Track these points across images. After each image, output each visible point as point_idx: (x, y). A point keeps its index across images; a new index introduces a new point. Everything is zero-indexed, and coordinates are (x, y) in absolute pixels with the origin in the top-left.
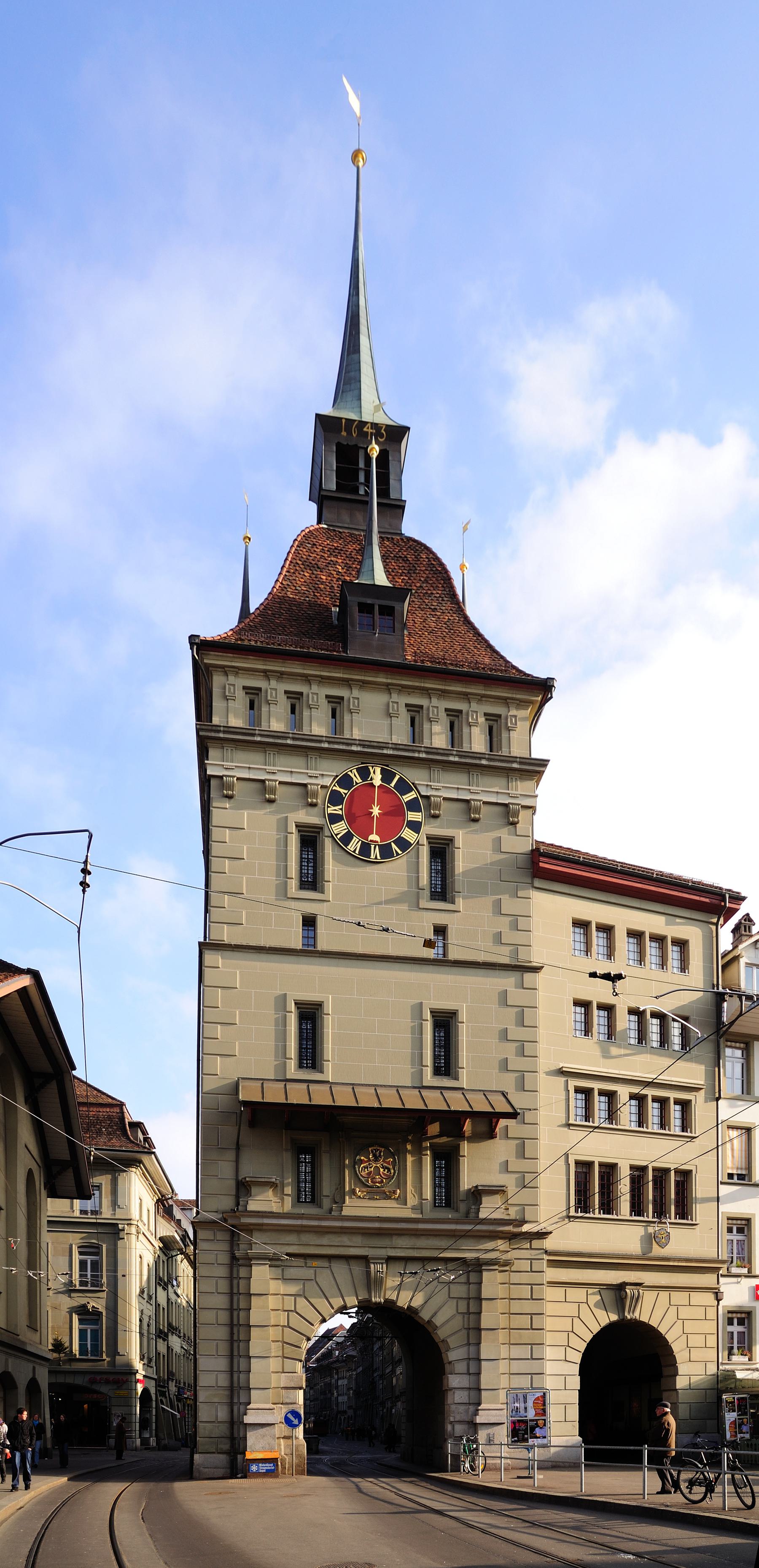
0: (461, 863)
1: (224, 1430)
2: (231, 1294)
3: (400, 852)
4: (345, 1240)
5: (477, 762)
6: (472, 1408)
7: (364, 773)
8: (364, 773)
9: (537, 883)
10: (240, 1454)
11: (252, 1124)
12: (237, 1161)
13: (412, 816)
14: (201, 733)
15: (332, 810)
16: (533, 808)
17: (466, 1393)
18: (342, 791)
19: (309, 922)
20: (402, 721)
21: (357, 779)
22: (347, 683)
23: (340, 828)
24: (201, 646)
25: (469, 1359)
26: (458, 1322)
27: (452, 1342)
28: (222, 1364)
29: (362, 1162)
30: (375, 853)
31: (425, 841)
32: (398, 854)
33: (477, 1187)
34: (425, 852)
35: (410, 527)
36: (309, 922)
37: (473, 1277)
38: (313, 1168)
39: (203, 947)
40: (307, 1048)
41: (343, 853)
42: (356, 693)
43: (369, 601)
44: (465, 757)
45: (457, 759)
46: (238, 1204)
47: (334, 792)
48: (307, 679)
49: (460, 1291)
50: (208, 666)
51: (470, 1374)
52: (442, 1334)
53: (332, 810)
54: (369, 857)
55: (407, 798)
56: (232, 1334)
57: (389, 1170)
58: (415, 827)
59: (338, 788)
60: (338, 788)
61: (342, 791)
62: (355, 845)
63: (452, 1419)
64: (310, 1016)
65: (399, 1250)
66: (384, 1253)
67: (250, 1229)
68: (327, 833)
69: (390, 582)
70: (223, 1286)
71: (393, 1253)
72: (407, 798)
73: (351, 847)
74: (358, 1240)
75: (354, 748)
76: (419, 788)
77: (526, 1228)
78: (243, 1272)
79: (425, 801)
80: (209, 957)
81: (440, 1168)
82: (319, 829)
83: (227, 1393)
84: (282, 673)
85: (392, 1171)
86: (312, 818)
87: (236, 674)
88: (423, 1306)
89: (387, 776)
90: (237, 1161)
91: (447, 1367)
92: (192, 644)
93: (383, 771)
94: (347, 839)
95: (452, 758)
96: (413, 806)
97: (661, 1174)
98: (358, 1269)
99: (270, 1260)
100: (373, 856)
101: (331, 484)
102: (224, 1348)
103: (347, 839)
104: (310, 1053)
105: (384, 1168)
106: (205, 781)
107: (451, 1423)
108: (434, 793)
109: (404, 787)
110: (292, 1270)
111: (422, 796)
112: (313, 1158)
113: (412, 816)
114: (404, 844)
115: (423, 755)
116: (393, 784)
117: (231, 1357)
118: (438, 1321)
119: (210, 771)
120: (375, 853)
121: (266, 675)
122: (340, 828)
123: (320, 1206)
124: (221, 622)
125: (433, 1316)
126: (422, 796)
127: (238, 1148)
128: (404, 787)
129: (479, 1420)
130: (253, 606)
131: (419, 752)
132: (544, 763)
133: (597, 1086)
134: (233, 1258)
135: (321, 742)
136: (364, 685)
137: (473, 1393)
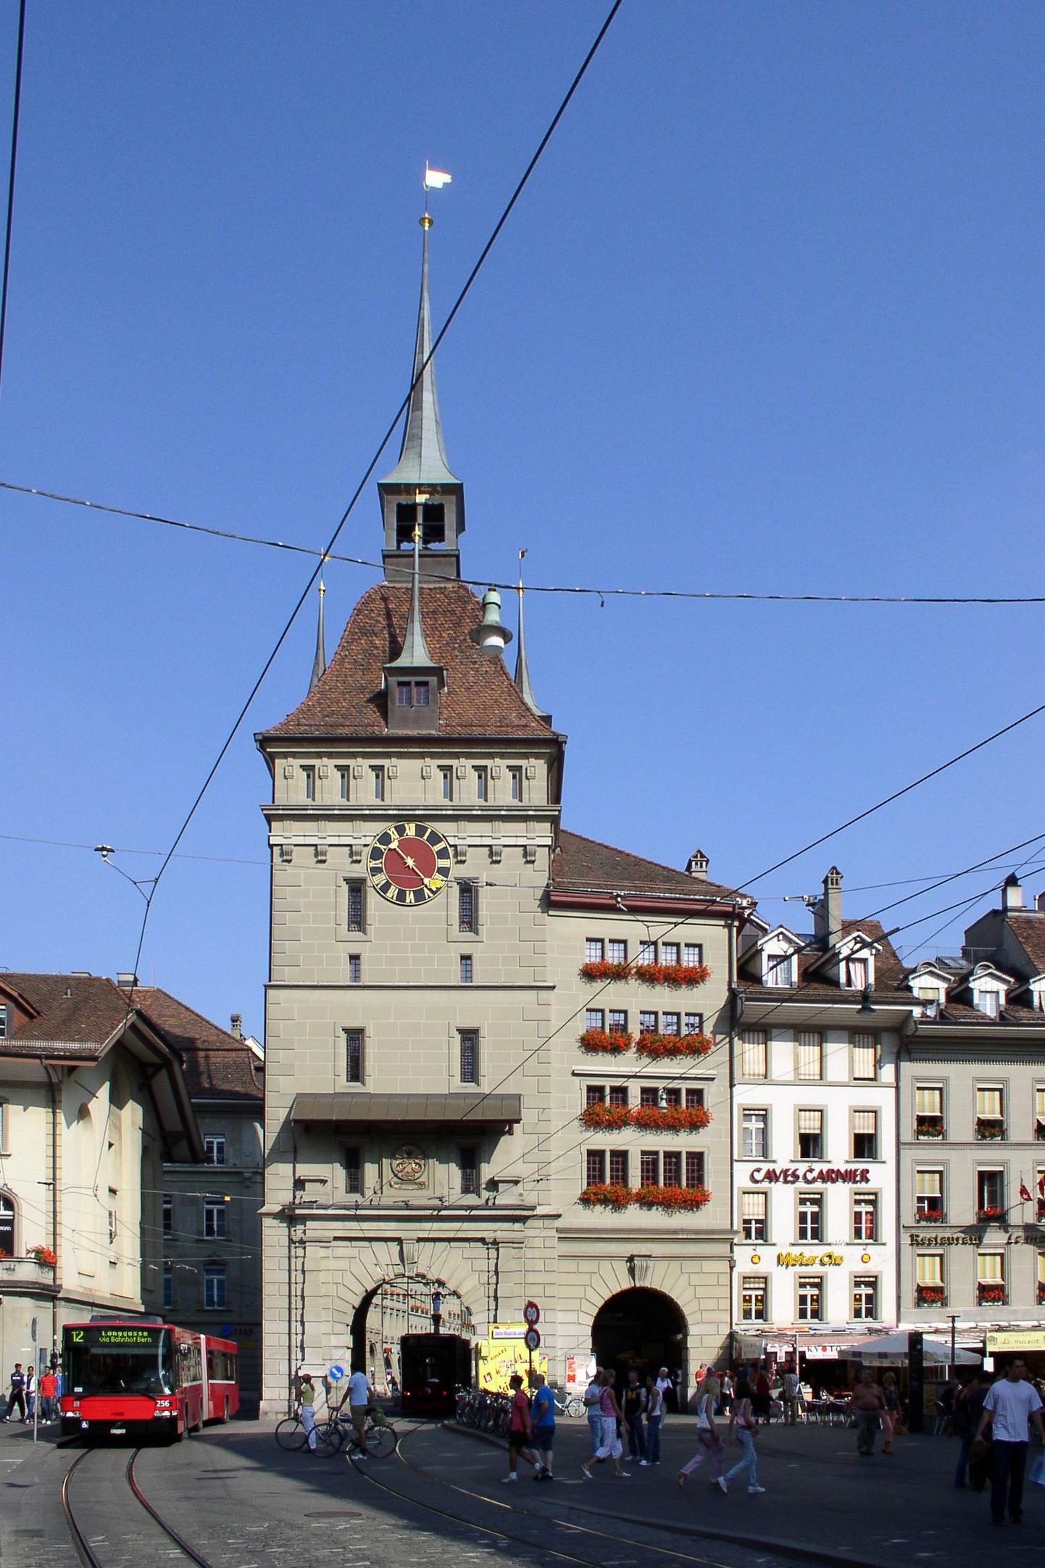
0: (485, 899)
4: (382, 1225)
7: (401, 830)
8: (401, 830)
13: (441, 863)
15: (373, 864)
19: (355, 958)
23: (381, 879)
30: (410, 898)
36: (355, 958)
49: (483, 1265)
53: (373, 864)
55: (436, 848)
58: (444, 872)
62: (393, 892)
64: (355, 1037)
67: (304, 1219)
68: (369, 883)
72: (436, 848)
73: (389, 895)
80: (270, 992)
82: (363, 881)
89: (420, 831)
94: (385, 888)
96: (443, 854)
98: (394, 1247)
103: (385, 888)
104: (356, 1070)
108: (461, 842)
113: (441, 863)
120: (410, 898)
122: (381, 879)
123: (363, 1195)
127: (295, 1151)
128: (435, 838)
134: (291, 1241)
136: (400, 756)
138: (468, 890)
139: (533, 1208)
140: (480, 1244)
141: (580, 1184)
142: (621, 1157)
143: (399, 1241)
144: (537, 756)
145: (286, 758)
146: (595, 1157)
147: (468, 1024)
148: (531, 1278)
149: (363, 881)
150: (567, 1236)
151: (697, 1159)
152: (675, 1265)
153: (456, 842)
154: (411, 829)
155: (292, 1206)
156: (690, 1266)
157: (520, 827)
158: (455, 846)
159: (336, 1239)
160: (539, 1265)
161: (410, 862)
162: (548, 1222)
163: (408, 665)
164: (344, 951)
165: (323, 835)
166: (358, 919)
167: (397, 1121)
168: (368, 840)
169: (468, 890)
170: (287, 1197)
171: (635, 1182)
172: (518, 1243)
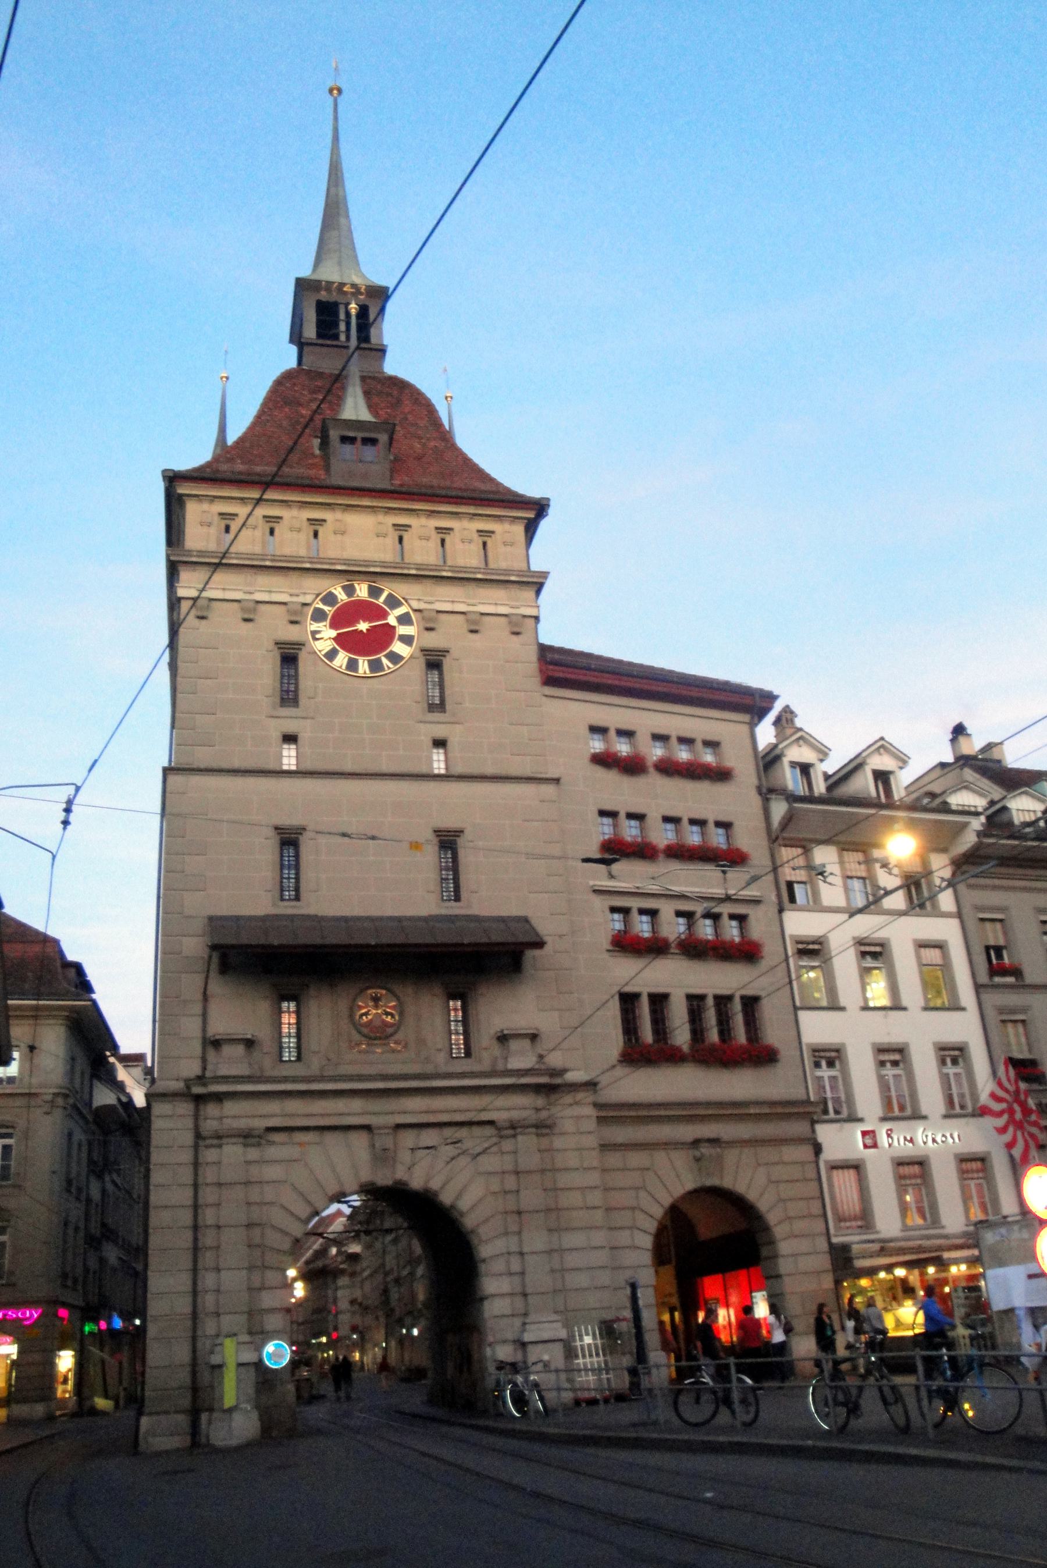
1: (184, 1376)
2: (196, 1186)
3: (391, 665)
6: (517, 1322)
8: (349, 590)
10: (207, 1410)
12: (204, 1015)
13: (403, 630)
14: (172, 558)
16: (537, 618)
17: (508, 1300)
18: (326, 608)
20: (391, 540)
21: (342, 596)
24: (172, 479)
25: (509, 1253)
27: (484, 1232)
28: (184, 1281)
29: (361, 1008)
31: (419, 654)
32: (389, 668)
33: (502, 1031)
34: (421, 663)
35: (393, 366)
37: (508, 1145)
38: (298, 1018)
39: (166, 771)
40: (289, 878)
41: (328, 669)
42: (338, 515)
43: (351, 434)
44: (458, 572)
46: (204, 1069)
47: (317, 610)
50: (181, 496)
51: (511, 1274)
52: (469, 1222)
54: (356, 670)
58: (407, 640)
59: (321, 606)
60: (321, 606)
65: (407, 1116)
69: (375, 417)
70: (186, 1175)
74: (357, 1104)
76: (411, 602)
78: (210, 1155)
79: (418, 614)
81: (456, 1010)
82: (300, 645)
85: (397, 1018)
86: (291, 634)
88: (442, 1188)
89: (374, 592)
90: (204, 1015)
91: (483, 1268)
92: (164, 477)
93: (370, 587)
95: (445, 574)
97: (722, 1001)
98: (359, 1141)
99: (245, 1137)
100: (361, 671)
101: (310, 332)
102: (186, 1262)
105: (387, 1014)
106: (174, 603)
109: (394, 602)
111: (415, 611)
112: (298, 1006)
113: (403, 630)
114: (395, 658)
115: (413, 572)
117: (195, 1271)
118: (464, 1205)
119: (181, 592)
124: (197, 454)
126: (415, 611)
129: (527, 1337)
130: (232, 438)
131: (409, 568)
132: (545, 575)
133: (635, 904)
134: (198, 1136)
135: (302, 562)
138: (434, 661)
139: (562, 1072)
140: (489, 1131)
141: (614, 1041)
142: (659, 1001)
143: (367, 1128)
145: (201, 501)
146: (628, 1000)
147: (449, 822)
149: (300, 645)
150: (612, 1114)
151: (751, 1003)
152: (747, 1153)
153: (422, 606)
154: (362, 591)
156: (768, 1154)
157: (498, 594)
158: (419, 611)
159: (269, 1129)
161: (363, 626)
162: (580, 1096)
163: (354, 418)
164: (276, 728)
165: (251, 589)
166: (289, 697)
168: (308, 599)
169: (434, 661)
170: (192, 1069)
171: (681, 1036)
172: (543, 1128)
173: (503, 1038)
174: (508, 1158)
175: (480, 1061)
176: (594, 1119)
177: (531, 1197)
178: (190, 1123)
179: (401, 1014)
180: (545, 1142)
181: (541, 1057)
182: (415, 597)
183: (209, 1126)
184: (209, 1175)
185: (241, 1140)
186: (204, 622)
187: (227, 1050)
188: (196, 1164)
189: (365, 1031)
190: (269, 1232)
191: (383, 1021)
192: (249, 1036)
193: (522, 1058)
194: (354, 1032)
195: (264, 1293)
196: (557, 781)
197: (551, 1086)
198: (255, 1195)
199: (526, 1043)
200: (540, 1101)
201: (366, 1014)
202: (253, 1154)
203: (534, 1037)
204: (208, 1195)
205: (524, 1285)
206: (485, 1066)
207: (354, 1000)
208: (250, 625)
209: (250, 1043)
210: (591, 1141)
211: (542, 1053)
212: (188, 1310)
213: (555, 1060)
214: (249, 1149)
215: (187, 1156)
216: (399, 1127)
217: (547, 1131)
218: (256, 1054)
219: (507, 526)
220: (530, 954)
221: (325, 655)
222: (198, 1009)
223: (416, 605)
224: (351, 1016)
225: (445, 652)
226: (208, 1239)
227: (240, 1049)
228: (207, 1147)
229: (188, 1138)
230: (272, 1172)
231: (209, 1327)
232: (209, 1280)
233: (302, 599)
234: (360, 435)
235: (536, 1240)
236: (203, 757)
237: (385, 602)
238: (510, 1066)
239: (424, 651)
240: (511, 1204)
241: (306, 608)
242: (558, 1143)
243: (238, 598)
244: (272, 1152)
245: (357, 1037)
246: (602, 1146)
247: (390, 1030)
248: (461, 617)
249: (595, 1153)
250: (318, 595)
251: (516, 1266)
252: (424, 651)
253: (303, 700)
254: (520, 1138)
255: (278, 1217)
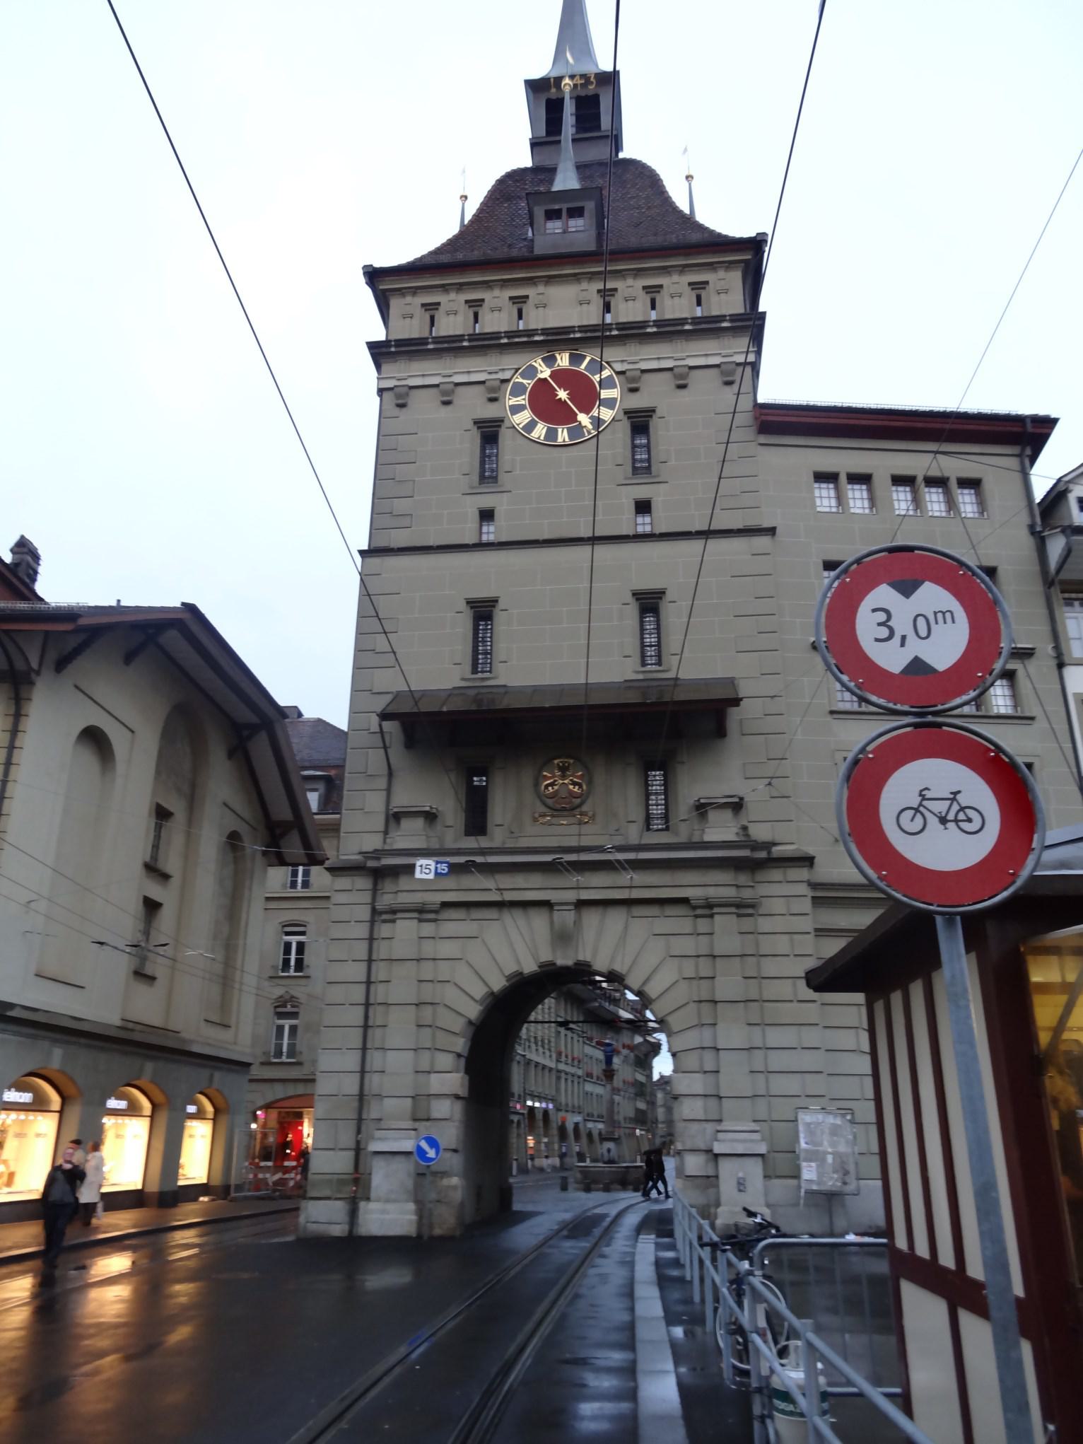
4: (519, 880)
5: (679, 328)
6: (710, 1127)
8: (550, 361)
9: (763, 439)
11: (411, 741)
12: (389, 790)
13: (605, 394)
15: (514, 401)
18: (525, 382)
22: (531, 281)
26: (682, 993)
28: (351, 1061)
29: (546, 778)
31: (621, 416)
37: (703, 925)
42: (541, 289)
43: (557, 207)
45: (655, 330)
48: (487, 285)
49: (687, 945)
50: (385, 291)
53: (514, 401)
54: (556, 439)
56: (366, 1017)
57: (580, 785)
60: (520, 380)
61: (525, 382)
63: (679, 1146)
65: (592, 891)
66: (571, 896)
68: (506, 424)
70: (361, 950)
71: (585, 895)
74: (536, 880)
75: (537, 338)
76: (615, 365)
77: (777, 851)
78: (384, 930)
79: (622, 377)
82: (498, 422)
83: (356, 1104)
84: (461, 285)
86: (490, 412)
87: (414, 294)
88: (629, 971)
89: (576, 359)
90: (389, 790)
93: (571, 355)
95: (649, 330)
98: (539, 921)
100: (560, 440)
102: (355, 1037)
105: (574, 784)
107: (679, 1153)
110: (450, 925)
111: (618, 373)
113: (605, 394)
116: (583, 366)
121: (445, 288)
125: (645, 983)
126: (618, 373)
127: (390, 774)
134: (375, 912)
136: (549, 280)
137: (713, 1102)
138: (640, 422)
143: (547, 904)
144: (729, 265)
147: (649, 583)
148: (770, 967)
149: (498, 422)
155: (377, 854)
159: (446, 905)
160: (782, 945)
167: (543, 709)
168: (507, 375)
169: (640, 422)
170: (373, 842)
172: (744, 908)
173: (702, 809)
174: (704, 940)
175: (677, 834)
176: (808, 901)
177: (729, 985)
178: (367, 897)
179: (590, 783)
180: (747, 924)
181: (745, 828)
182: (620, 357)
183: (386, 900)
184: (382, 950)
185: (415, 915)
186: (404, 410)
187: (406, 824)
188: (371, 939)
189: (549, 802)
190: (440, 1009)
191: (570, 792)
192: (427, 809)
193: (721, 829)
194: (538, 803)
195: (433, 1076)
196: (772, 531)
197: (756, 860)
198: (427, 971)
199: (728, 814)
200: (743, 879)
201: (552, 785)
202: (428, 929)
203: (737, 806)
204: (380, 971)
205: (717, 1086)
206: (682, 838)
207: (540, 771)
208: (449, 408)
209: (430, 817)
210: (807, 924)
211: (745, 823)
212: (355, 1090)
213: (760, 833)
214: (425, 924)
215: (363, 931)
216: (581, 904)
217: (750, 911)
218: (439, 826)
219: (721, 274)
220: (734, 714)
221: (523, 428)
222: (383, 783)
223: (619, 367)
224: (537, 785)
225: (650, 412)
226: (377, 1016)
227: (419, 823)
228: (385, 921)
229: (365, 913)
230: (447, 949)
231: (373, 1112)
232: (375, 1060)
233: (502, 376)
234: (564, 206)
235: (732, 1033)
236: (400, 538)
237: (586, 369)
238: (707, 838)
239: (629, 413)
240: (704, 991)
241: (504, 385)
242: (764, 924)
243: (436, 382)
244: (449, 928)
245: (543, 809)
246: (816, 930)
247: (578, 801)
248: (667, 375)
249: (810, 937)
250: (517, 370)
251: (709, 1061)
252: (629, 413)
253: (503, 477)
254: (717, 917)
255: (450, 995)
